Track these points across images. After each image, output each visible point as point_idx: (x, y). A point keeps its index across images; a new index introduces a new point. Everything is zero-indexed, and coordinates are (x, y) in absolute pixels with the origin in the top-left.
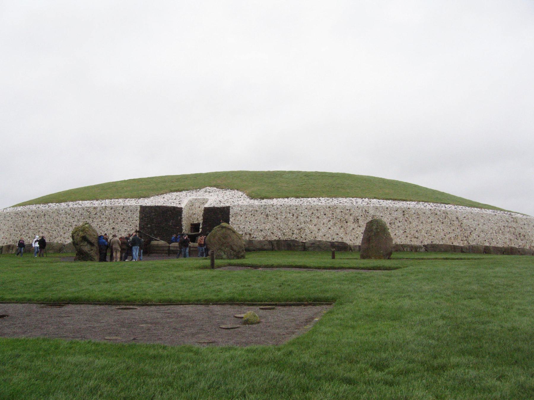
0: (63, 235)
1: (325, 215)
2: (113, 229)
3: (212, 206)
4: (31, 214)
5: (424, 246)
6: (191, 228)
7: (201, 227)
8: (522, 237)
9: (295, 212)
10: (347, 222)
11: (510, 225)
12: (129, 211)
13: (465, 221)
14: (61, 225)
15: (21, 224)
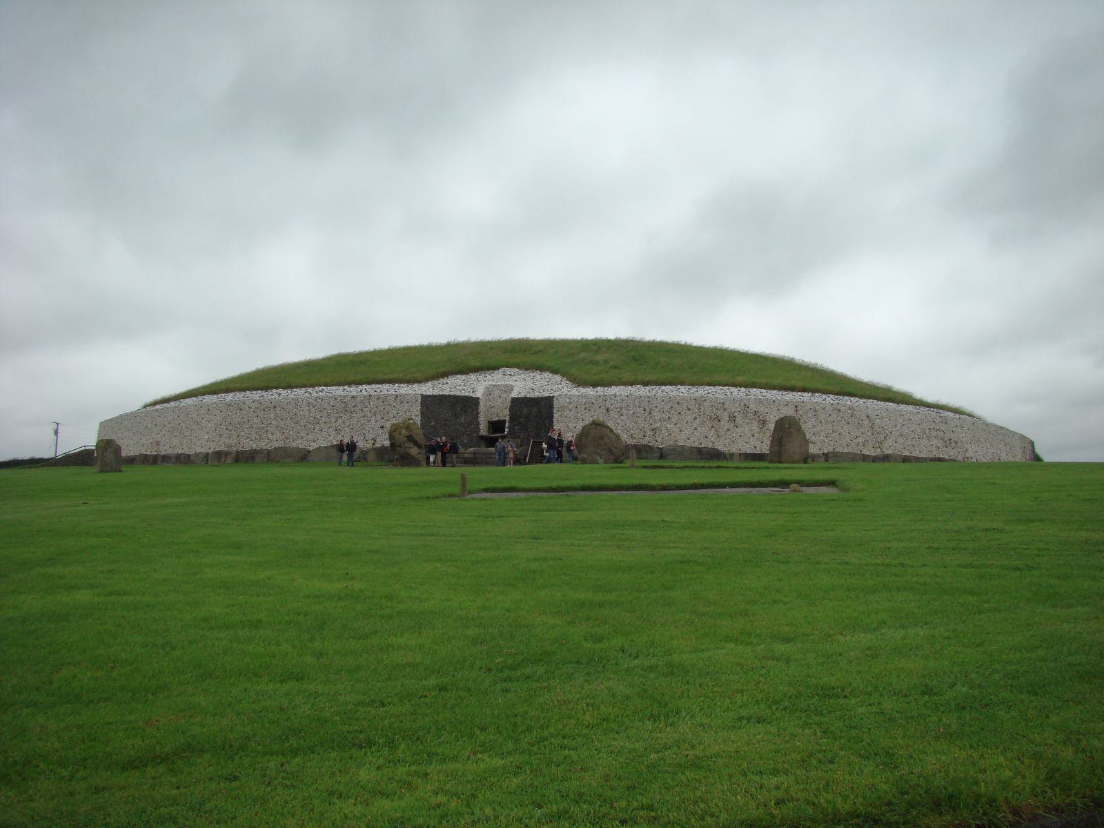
0: (305, 437)
1: (689, 409)
2: (382, 427)
3: (522, 395)
4: (253, 406)
5: (823, 454)
6: (489, 427)
7: (507, 425)
8: (953, 444)
9: (648, 407)
10: (719, 421)
11: (938, 427)
12: (405, 403)
13: (877, 420)
14: (303, 422)
15: (236, 421)
